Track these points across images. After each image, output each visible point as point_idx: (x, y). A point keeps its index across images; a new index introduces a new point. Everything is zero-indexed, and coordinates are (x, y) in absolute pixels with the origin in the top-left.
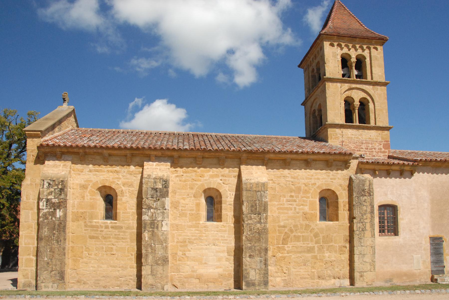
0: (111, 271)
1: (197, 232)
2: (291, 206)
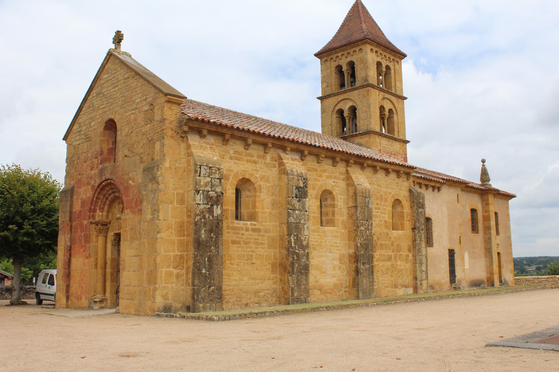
0: (251, 285)
1: (318, 237)
2: (378, 214)
